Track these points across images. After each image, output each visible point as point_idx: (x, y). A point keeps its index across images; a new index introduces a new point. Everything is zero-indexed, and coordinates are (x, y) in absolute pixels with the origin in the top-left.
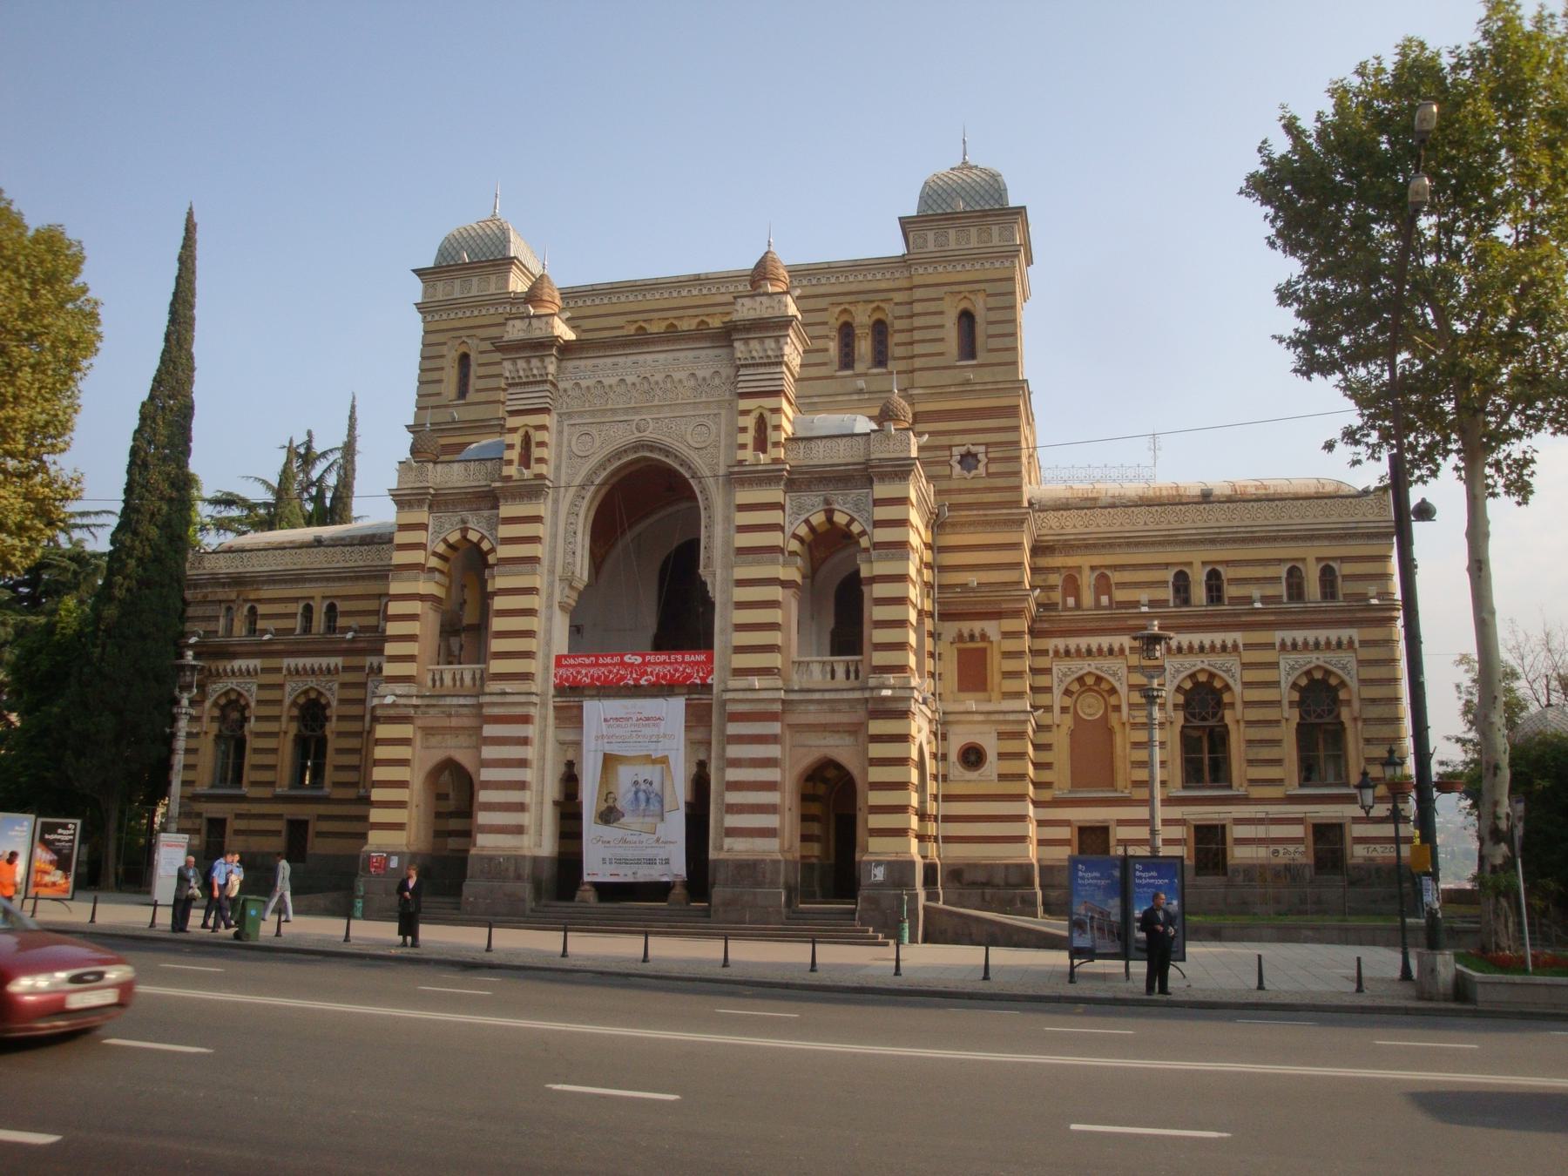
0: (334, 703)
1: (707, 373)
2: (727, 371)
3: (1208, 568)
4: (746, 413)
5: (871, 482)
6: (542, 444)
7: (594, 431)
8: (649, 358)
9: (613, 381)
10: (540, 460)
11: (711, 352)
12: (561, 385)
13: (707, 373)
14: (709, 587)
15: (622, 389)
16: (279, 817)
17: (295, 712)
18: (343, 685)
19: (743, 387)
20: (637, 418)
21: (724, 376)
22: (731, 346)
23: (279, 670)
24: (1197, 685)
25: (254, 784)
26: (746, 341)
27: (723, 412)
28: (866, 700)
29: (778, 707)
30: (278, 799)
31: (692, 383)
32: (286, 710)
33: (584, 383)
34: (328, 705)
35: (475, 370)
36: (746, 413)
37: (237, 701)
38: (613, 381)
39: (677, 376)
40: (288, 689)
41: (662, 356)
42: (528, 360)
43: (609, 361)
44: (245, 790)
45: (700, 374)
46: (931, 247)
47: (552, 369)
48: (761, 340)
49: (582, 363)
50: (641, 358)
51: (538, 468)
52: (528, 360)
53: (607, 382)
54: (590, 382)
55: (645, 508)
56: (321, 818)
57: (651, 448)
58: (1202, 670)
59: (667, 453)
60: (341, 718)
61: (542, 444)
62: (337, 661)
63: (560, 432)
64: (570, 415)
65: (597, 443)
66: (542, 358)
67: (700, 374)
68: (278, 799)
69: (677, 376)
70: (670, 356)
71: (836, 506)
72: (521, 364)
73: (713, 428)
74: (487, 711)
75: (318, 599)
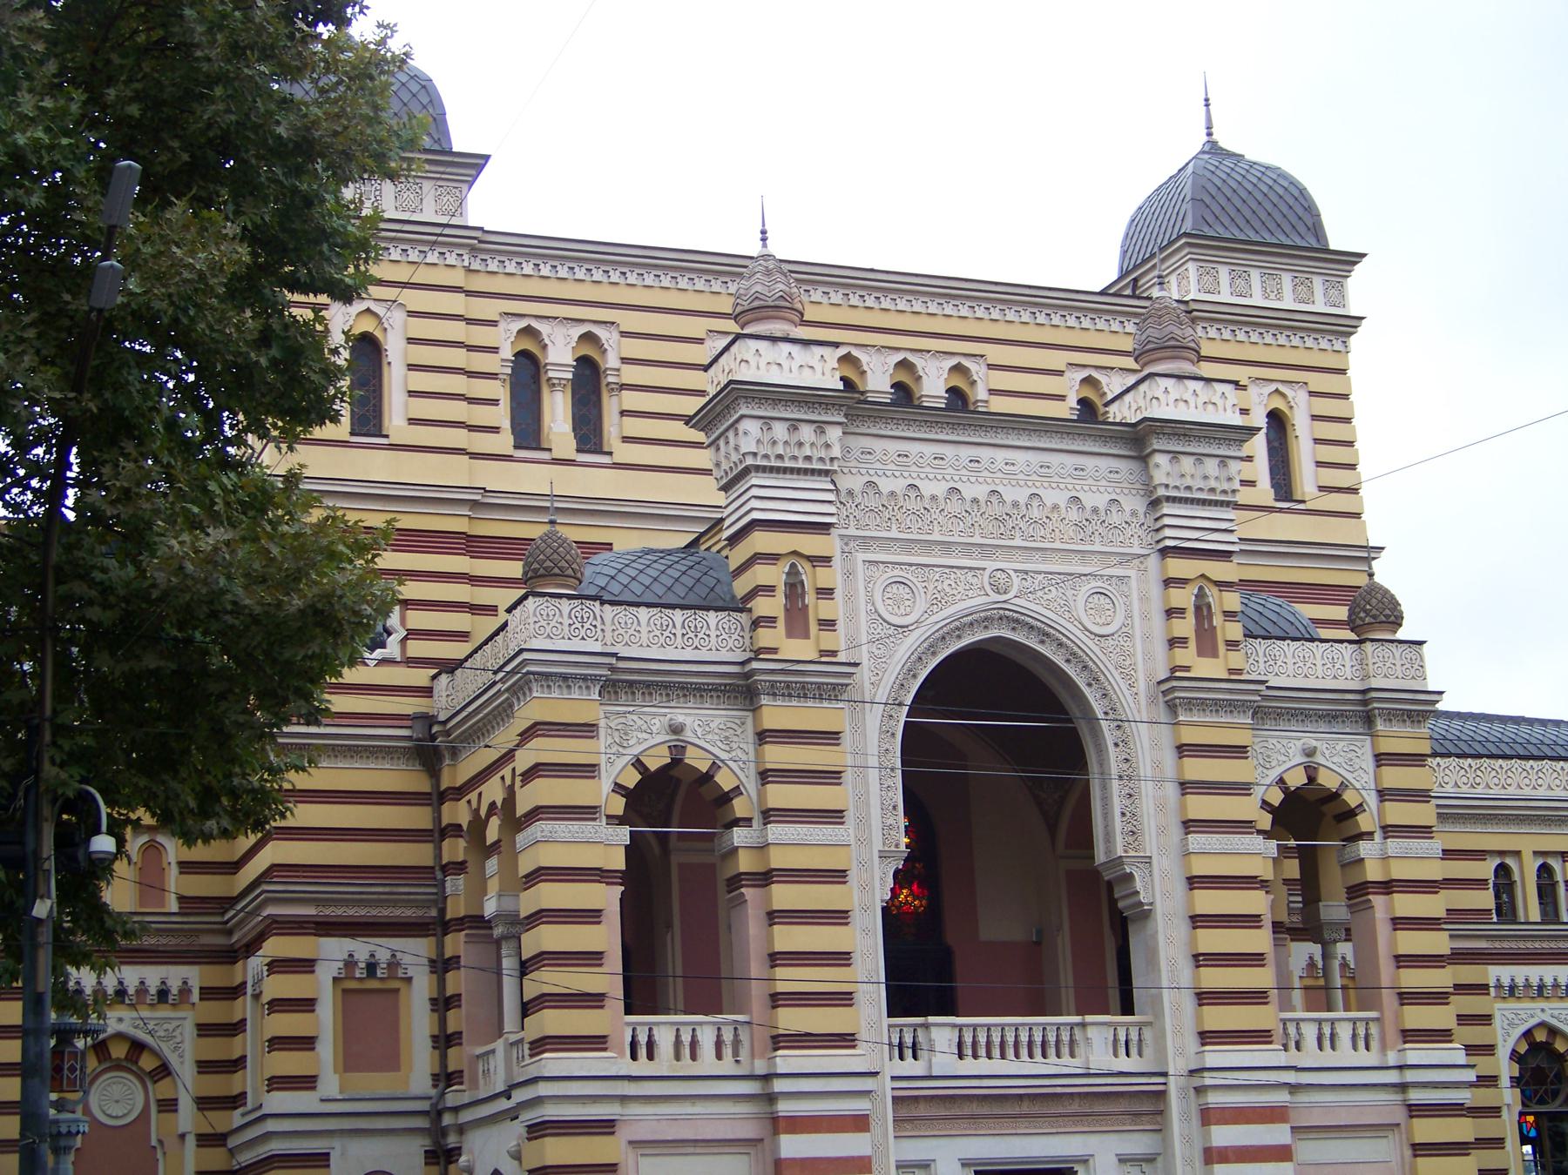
1: (1101, 501)
2: (1134, 503)
3: (1540, 861)
4: (1183, 582)
5: (1368, 720)
6: (826, 593)
7: (908, 575)
8: (1001, 455)
9: (940, 489)
10: (828, 624)
11: (1104, 464)
12: (845, 483)
13: (1101, 501)
14: (1139, 885)
15: (954, 507)
19: (1172, 538)
20: (991, 565)
21: (1127, 509)
22: (1143, 459)
24: (1534, 1047)
26: (1175, 455)
27: (1132, 573)
28: (1403, 1087)
29: (1282, 1097)
31: (1074, 515)
33: (886, 485)
35: (396, 379)
36: (1183, 582)
38: (940, 489)
39: (1051, 497)
41: (1019, 457)
42: (794, 425)
43: (929, 450)
45: (1089, 500)
46: (1225, 296)
47: (836, 451)
48: (1200, 457)
49: (878, 445)
50: (985, 454)
51: (827, 640)
52: (794, 425)
53: (928, 488)
54: (899, 485)
55: (998, 733)
57: (1015, 623)
58: (1542, 1024)
59: (1044, 636)
61: (826, 593)
63: (849, 574)
64: (866, 543)
65: (921, 604)
66: (820, 427)
67: (1089, 500)
69: (1051, 497)
70: (1030, 456)
71: (1319, 759)
72: (780, 430)
73: (1119, 601)
74: (785, 1108)
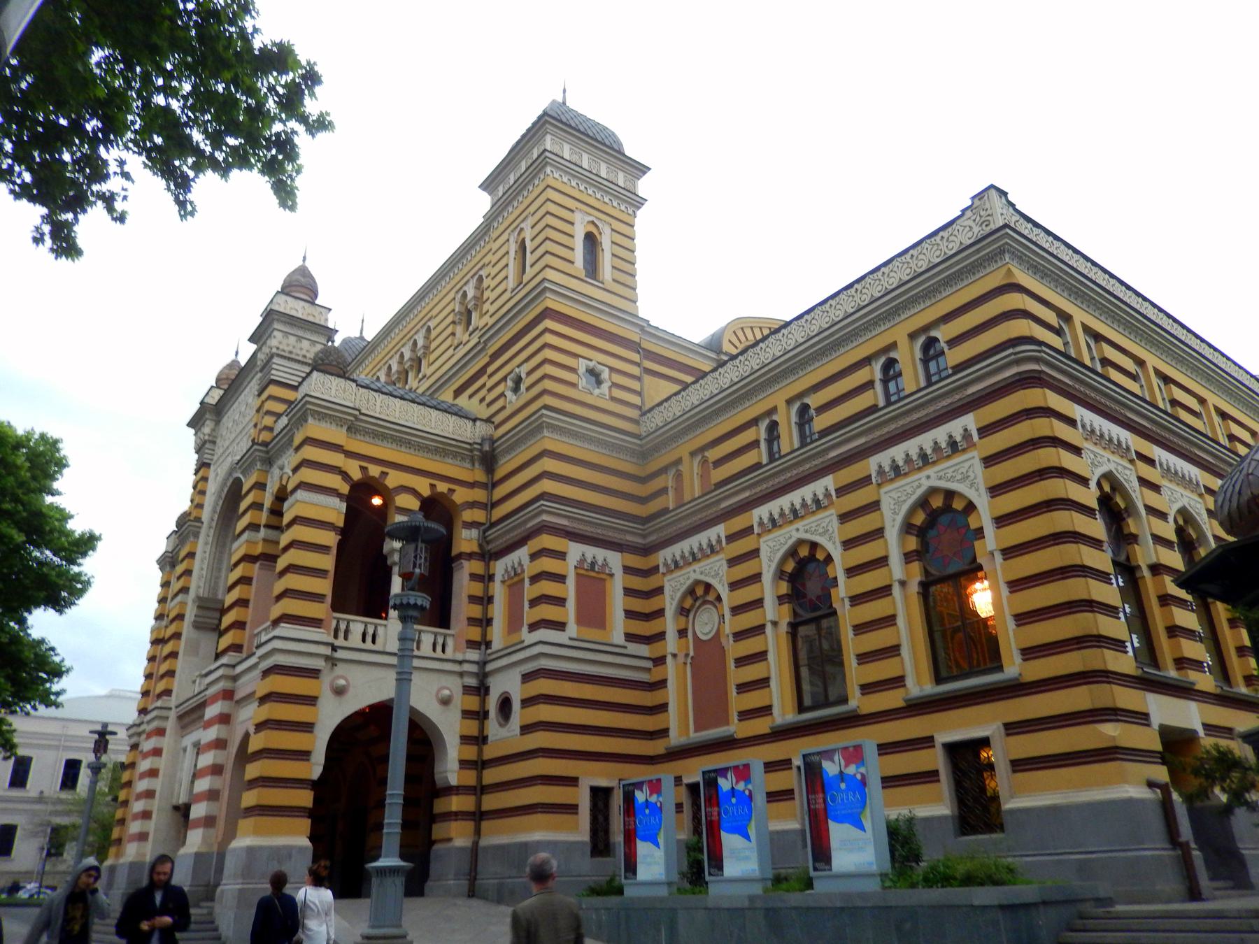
0: (982, 501)
16: (927, 742)
17: (913, 543)
18: (989, 461)
23: (866, 480)
25: (867, 688)
30: (917, 707)
32: (894, 544)
34: (971, 507)
37: (812, 558)
40: (885, 506)
44: (857, 702)
56: (1012, 728)
60: (1002, 521)
62: (969, 421)
68: (917, 707)
75: (903, 342)
